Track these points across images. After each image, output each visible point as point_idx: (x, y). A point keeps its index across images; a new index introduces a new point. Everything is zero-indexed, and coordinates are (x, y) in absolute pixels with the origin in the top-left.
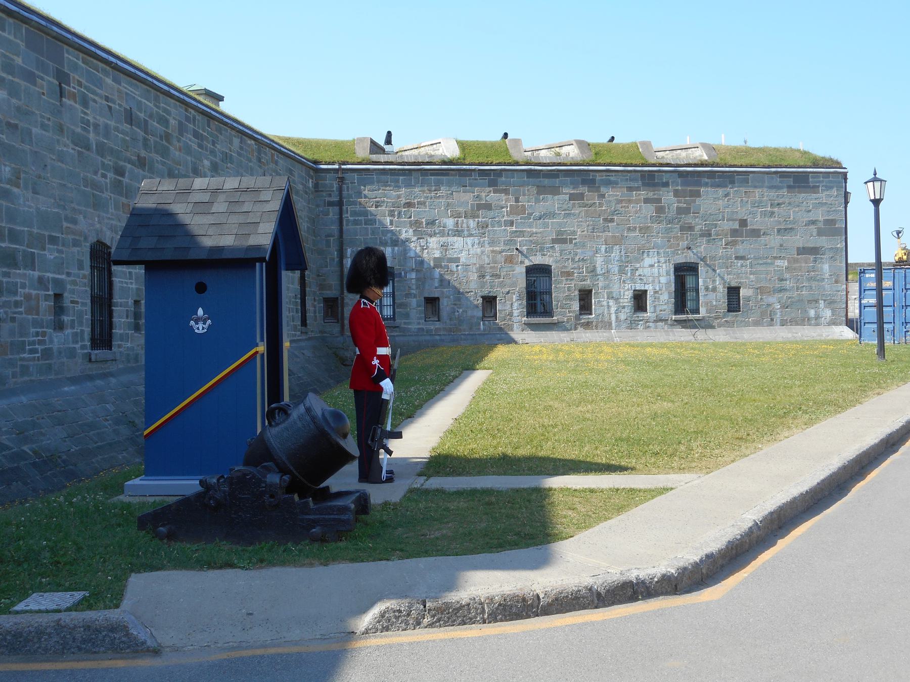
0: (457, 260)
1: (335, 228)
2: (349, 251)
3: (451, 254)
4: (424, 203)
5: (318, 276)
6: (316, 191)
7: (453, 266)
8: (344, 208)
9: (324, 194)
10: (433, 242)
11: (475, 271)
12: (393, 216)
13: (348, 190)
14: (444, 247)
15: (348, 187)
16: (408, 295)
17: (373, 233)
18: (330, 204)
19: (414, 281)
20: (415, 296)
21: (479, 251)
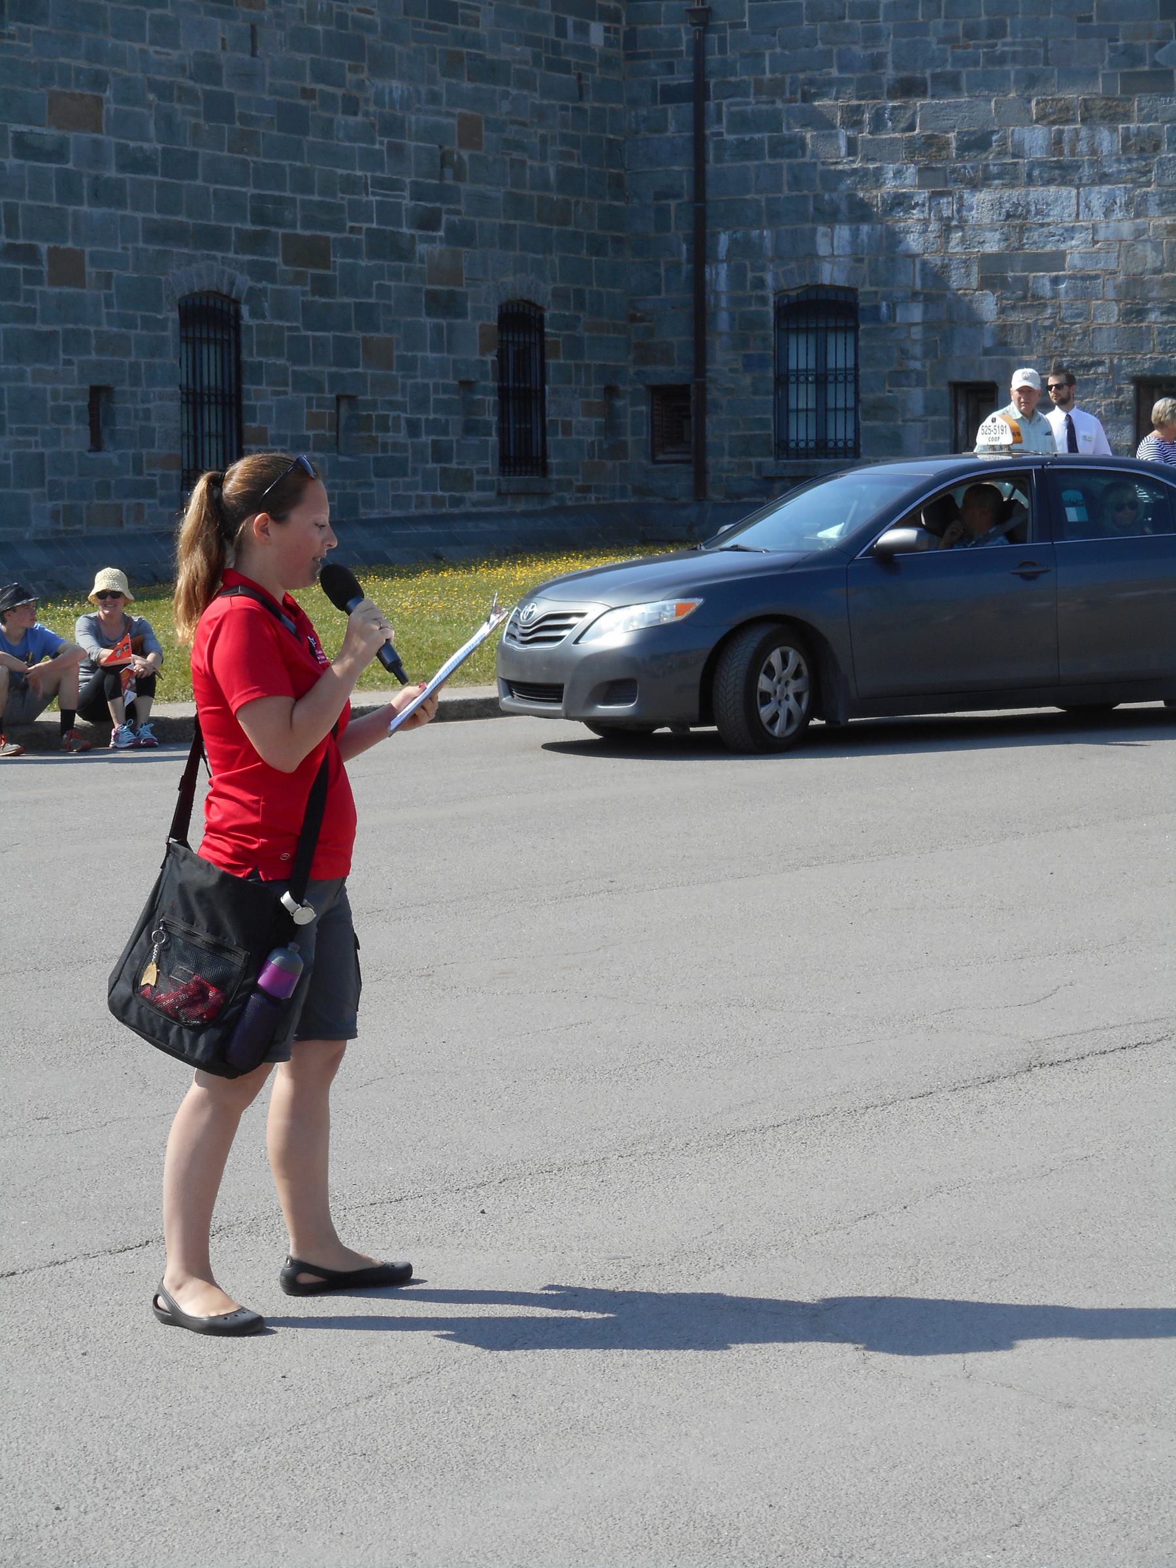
0: (1057, 259)
1: (681, 170)
2: (724, 239)
3: (1037, 242)
4: (951, 84)
5: (633, 319)
6: (630, 57)
7: (1042, 281)
8: (711, 105)
9: (653, 65)
10: (982, 204)
11: (1111, 294)
12: (857, 124)
13: (722, 50)
14: (1016, 219)
15: (722, 40)
16: (900, 377)
17: (796, 182)
18: (670, 95)
19: (917, 333)
20: (920, 380)
21: (1127, 228)
